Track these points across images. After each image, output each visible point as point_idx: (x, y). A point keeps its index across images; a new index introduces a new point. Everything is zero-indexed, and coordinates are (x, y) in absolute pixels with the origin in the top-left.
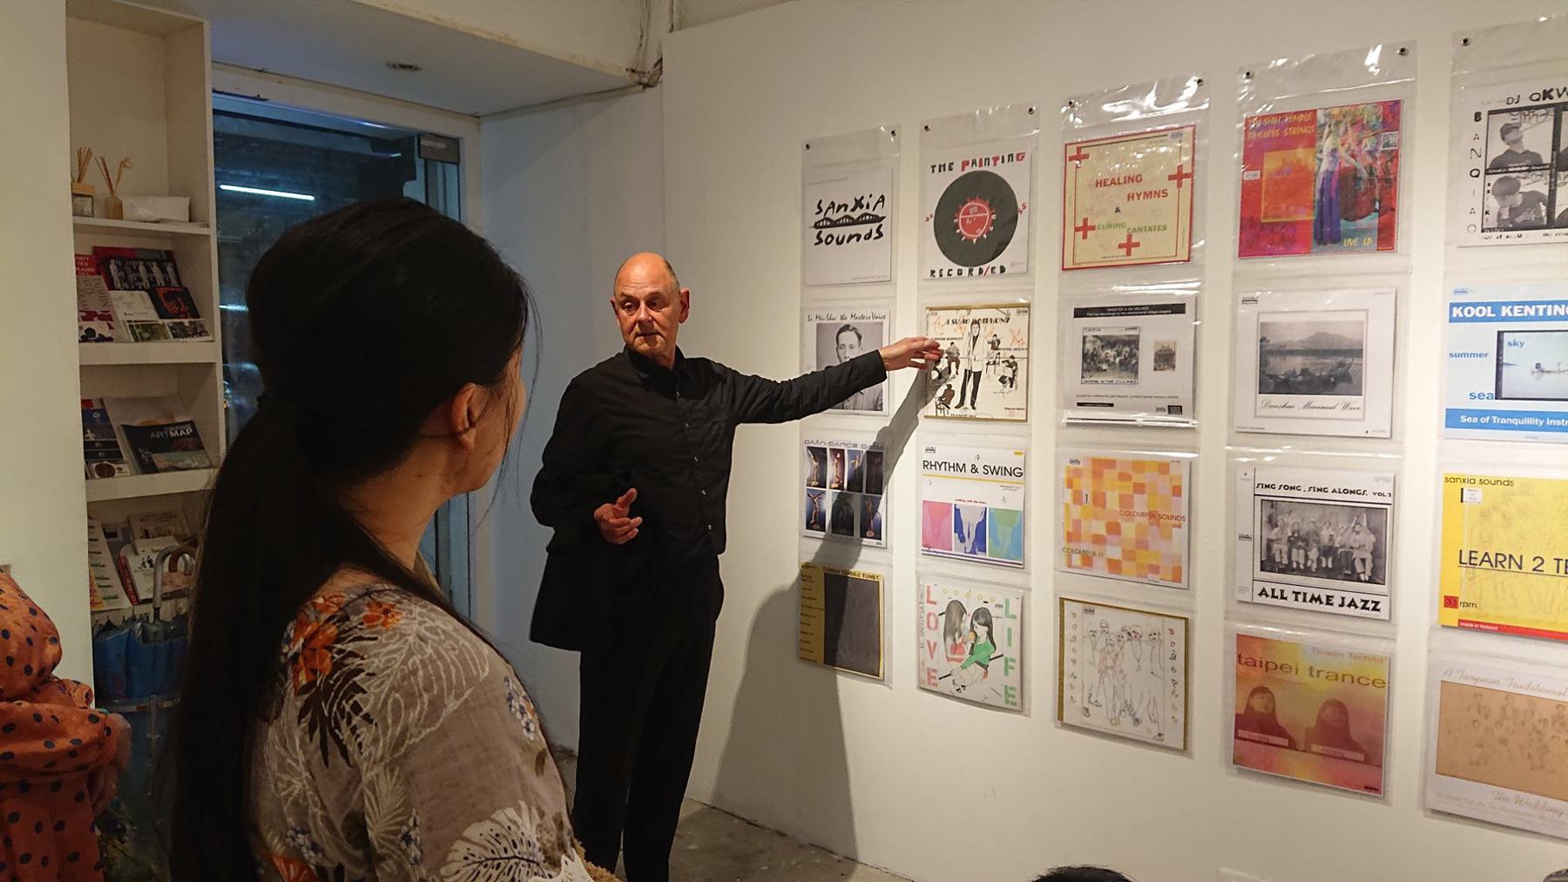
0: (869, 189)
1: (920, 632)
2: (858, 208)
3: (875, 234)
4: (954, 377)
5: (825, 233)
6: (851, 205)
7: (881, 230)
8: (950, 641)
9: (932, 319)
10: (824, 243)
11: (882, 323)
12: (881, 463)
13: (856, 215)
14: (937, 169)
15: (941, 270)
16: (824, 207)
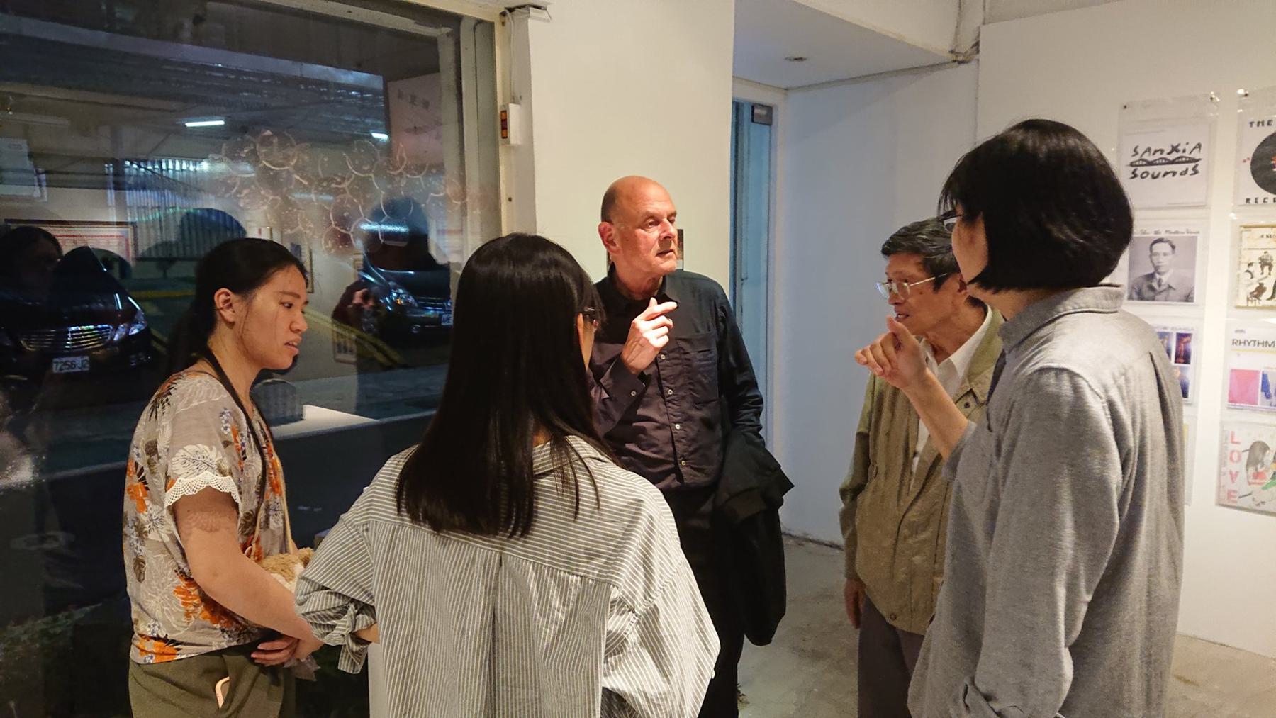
0: (1186, 139)
1: (1222, 463)
2: (1175, 152)
3: (1190, 171)
4: (1266, 277)
5: (1140, 170)
6: (1168, 149)
7: (1197, 168)
8: (1252, 470)
9: (1246, 234)
10: (1139, 178)
11: (1196, 237)
12: (1188, 342)
13: (1171, 157)
14: (1255, 125)
15: (1256, 199)
16: (1140, 151)
